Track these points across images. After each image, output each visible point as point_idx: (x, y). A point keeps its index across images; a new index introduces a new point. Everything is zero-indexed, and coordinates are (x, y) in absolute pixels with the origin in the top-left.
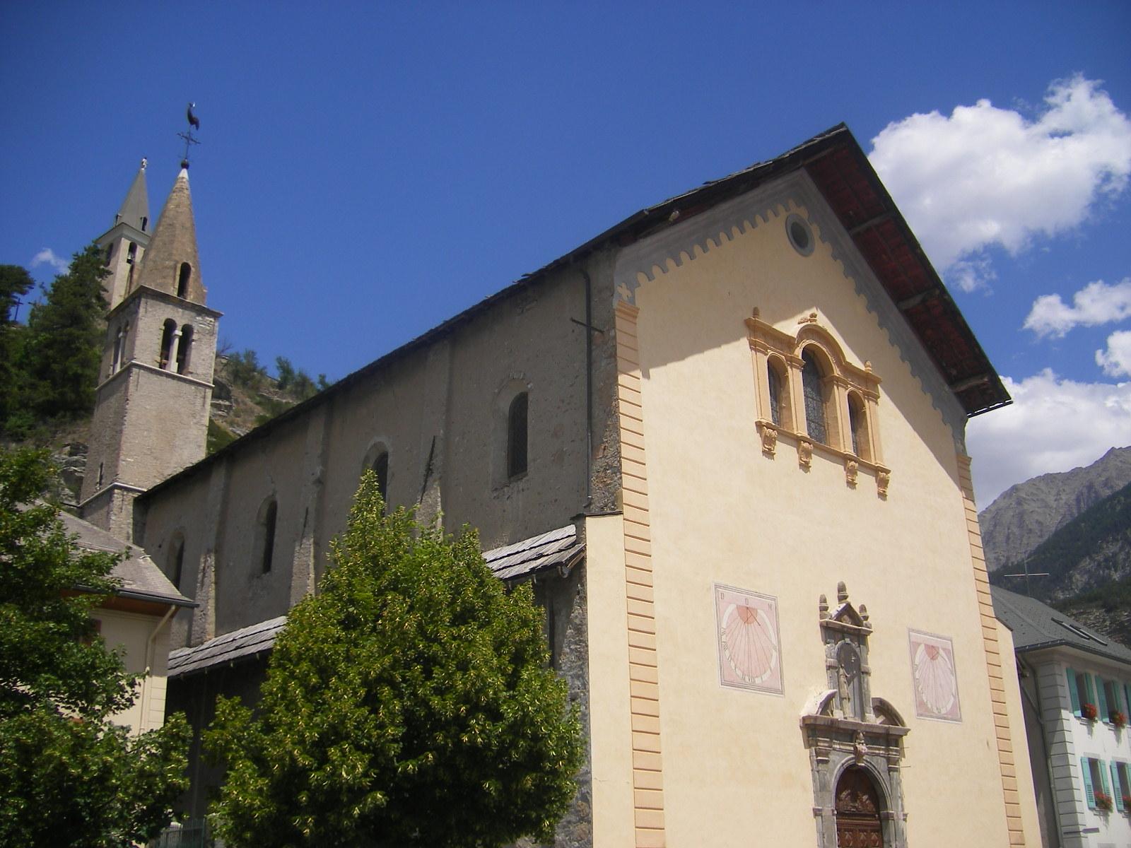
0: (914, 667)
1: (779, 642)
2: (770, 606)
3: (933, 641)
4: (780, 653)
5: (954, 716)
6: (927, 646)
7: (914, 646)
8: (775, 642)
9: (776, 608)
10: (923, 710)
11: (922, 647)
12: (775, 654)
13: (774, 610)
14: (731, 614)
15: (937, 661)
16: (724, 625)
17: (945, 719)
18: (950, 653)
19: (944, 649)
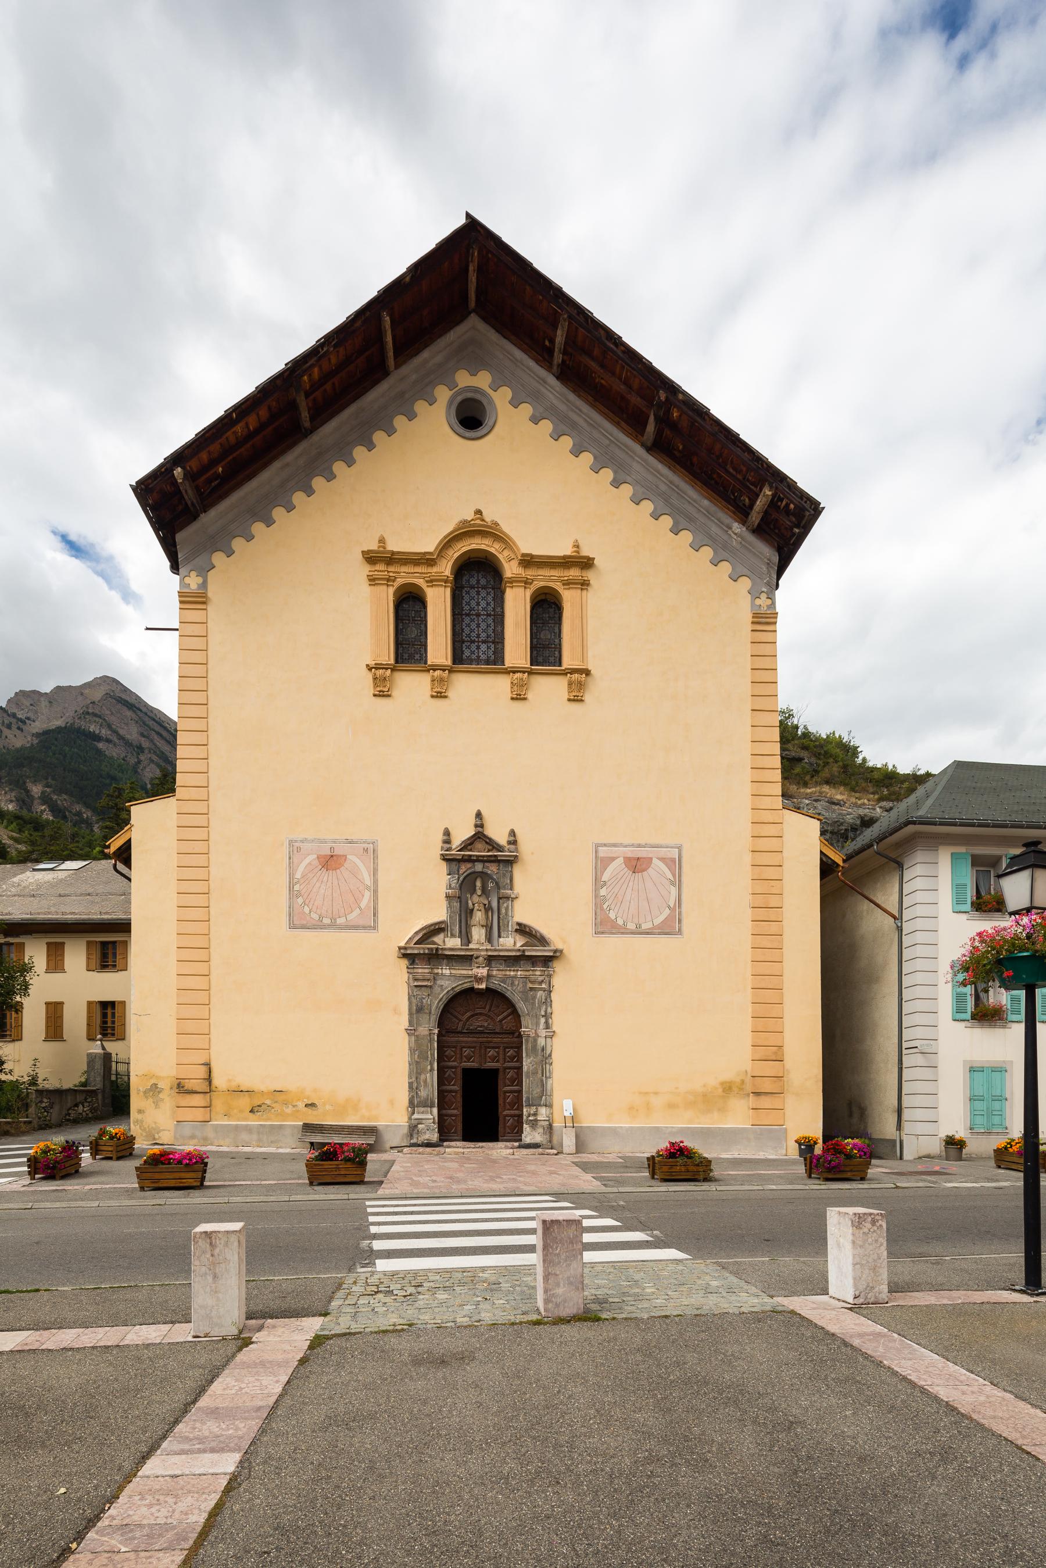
0: (598, 883)
1: (376, 882)
2: (366, 850)
3: (630, 852)
4: (376, 891)
5: (671, 927)
6: (628, 861)
7: (601, 863)
8: (368, 881)
9: (374, 851)
10: (604, 926)
11: (621, 860)
12: (367, 894)
13: (371, 851)
14: (310, 864)
15: (650, 870)
16: (298, 875)
17: (648, 933)
18: (676, 865)
19: (662, 859)
